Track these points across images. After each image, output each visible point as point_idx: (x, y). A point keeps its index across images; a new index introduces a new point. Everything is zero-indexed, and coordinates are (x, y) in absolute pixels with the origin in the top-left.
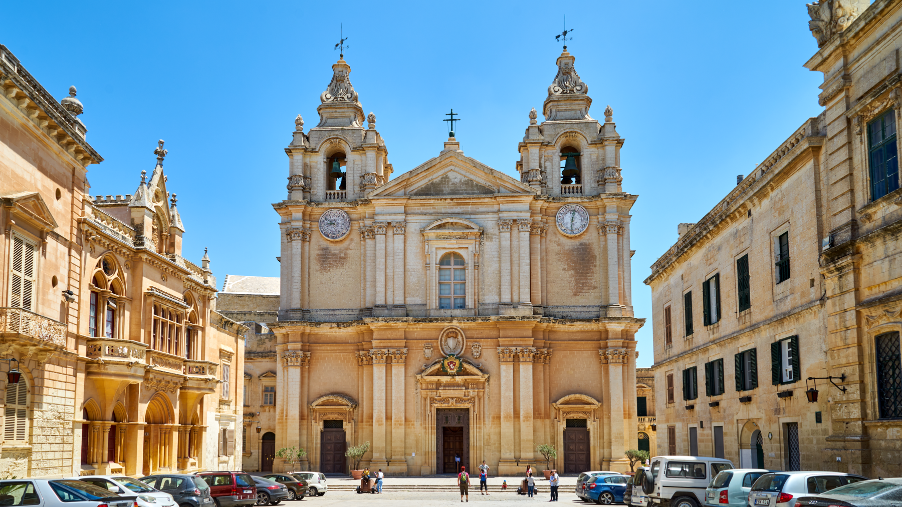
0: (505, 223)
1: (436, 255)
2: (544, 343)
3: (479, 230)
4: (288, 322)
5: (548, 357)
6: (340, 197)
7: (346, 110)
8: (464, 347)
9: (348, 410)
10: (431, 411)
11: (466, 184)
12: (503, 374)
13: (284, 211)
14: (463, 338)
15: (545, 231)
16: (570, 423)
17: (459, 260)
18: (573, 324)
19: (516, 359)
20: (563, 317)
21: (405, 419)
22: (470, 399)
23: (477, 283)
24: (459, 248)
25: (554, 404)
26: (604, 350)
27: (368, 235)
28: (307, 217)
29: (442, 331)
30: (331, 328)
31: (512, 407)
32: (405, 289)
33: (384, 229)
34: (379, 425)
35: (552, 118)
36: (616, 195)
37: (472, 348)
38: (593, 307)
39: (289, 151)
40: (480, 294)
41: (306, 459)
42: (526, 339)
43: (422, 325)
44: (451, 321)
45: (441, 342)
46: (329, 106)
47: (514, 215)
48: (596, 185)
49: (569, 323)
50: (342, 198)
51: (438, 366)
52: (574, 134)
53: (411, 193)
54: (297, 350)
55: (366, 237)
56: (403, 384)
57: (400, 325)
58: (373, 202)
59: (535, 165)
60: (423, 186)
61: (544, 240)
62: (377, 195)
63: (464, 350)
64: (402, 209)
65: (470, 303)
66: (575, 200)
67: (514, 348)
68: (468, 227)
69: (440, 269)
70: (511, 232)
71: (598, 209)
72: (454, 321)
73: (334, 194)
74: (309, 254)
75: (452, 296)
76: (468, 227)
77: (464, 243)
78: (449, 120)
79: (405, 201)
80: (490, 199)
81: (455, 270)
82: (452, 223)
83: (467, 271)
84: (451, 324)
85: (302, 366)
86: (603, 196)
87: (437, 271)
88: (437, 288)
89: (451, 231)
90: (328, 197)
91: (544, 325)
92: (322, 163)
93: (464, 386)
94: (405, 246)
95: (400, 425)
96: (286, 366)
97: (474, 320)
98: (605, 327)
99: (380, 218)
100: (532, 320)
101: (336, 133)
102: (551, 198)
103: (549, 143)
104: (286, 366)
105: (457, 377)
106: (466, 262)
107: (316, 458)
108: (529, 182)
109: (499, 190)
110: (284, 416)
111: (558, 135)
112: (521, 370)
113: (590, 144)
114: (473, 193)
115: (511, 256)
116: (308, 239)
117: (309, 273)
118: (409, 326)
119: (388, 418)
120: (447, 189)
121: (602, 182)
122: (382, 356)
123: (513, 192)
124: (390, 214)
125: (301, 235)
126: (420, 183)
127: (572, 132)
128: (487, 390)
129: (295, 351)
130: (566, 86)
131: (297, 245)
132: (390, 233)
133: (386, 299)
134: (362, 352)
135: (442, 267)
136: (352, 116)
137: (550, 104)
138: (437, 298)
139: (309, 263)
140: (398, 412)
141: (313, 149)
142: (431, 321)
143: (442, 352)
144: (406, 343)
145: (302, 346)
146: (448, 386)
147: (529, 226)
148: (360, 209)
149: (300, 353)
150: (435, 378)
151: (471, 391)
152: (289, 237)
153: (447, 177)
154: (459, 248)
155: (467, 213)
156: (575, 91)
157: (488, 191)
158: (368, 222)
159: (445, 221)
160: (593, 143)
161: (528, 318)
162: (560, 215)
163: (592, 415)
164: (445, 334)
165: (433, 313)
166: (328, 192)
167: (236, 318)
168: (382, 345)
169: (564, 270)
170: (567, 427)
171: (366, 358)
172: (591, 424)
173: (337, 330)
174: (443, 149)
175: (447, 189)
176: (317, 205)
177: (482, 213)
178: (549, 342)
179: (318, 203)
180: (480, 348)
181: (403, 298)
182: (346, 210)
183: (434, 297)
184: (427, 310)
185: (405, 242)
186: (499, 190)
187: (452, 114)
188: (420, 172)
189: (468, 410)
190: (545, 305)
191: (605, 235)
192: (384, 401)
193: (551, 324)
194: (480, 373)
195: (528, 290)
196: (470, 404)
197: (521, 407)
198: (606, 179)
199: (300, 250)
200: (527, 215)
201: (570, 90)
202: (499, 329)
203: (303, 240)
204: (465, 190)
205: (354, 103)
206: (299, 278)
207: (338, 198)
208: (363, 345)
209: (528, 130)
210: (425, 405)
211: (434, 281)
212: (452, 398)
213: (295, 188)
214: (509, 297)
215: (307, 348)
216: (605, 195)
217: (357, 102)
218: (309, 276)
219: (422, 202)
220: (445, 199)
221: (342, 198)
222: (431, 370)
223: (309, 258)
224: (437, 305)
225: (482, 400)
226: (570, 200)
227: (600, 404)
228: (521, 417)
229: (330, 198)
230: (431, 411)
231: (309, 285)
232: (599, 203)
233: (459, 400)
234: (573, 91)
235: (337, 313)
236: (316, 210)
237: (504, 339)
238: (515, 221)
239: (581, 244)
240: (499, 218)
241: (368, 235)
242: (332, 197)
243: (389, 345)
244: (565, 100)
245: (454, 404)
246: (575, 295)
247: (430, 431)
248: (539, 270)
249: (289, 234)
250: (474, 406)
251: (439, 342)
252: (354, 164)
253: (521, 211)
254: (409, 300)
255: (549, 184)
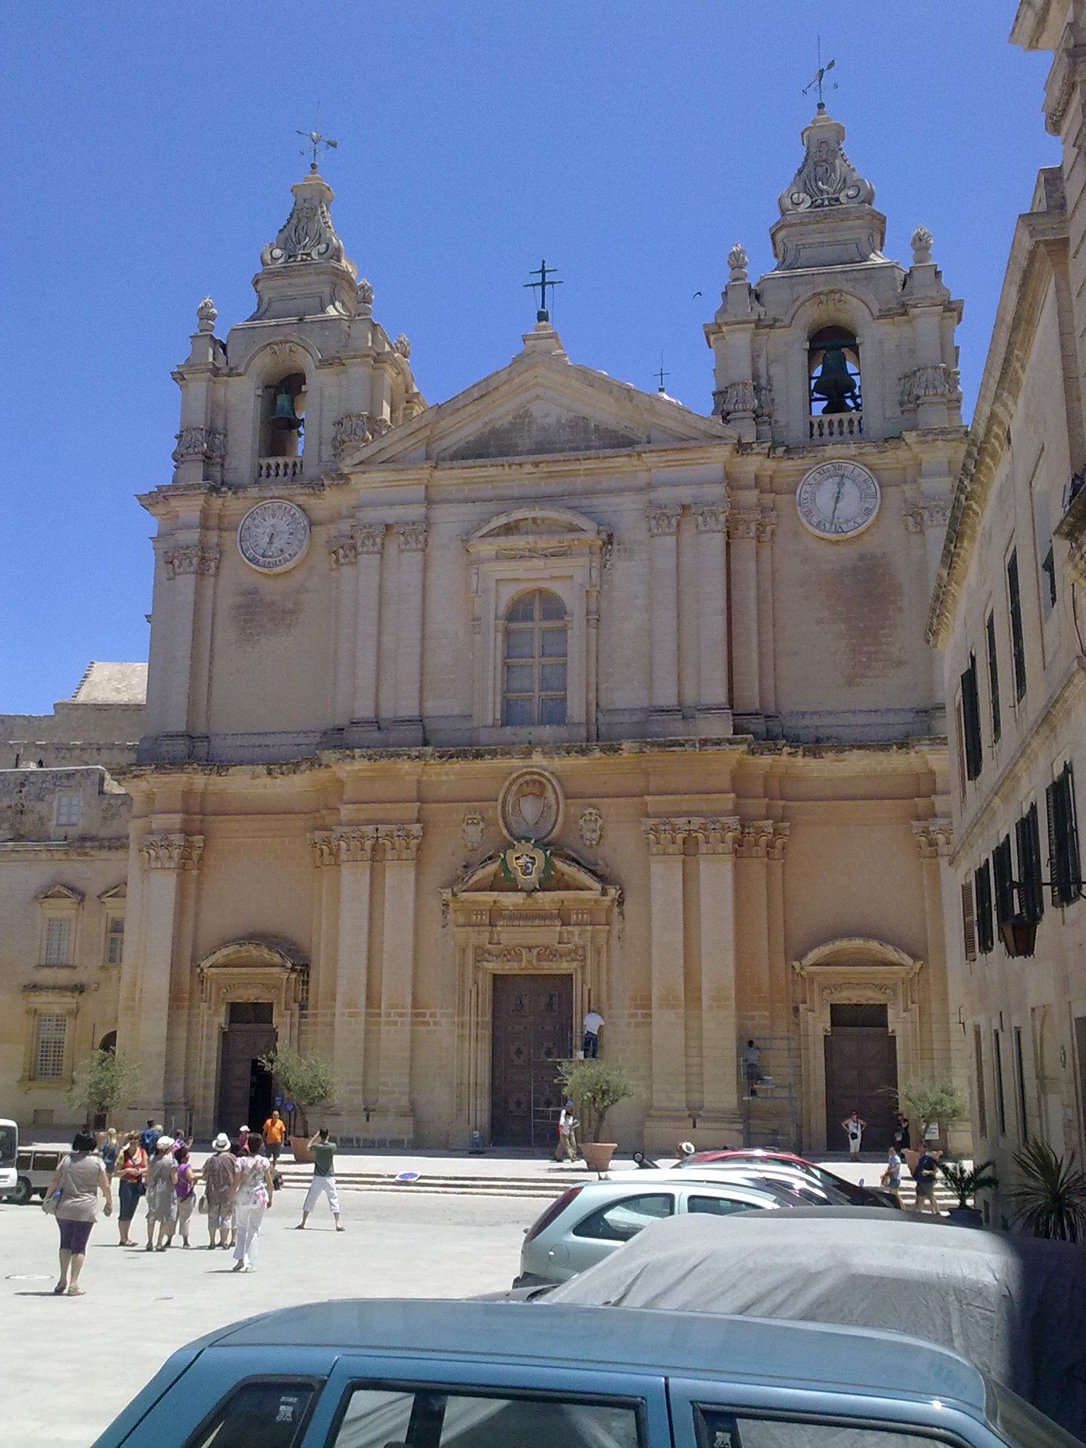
0: (664, 514)
1: (497, 597)
2: (768, 807)
3: (598, 533)
4: (151, 765)
5: (779, 843)
6: (290, 471)
7: (312, 279)
8: (560, 819)
9: (285, 976)
10: (476, 982)
11: (570, 427)
12: (657, 885)
13: (161, 509)
14: (557, 798)
15: (768, 529)
16: (841, 1016)
17: (553, 608)
18: (841, 756)
19: (689, 848)
20: (818, 740)
21: (414, 999)
22: (575, 951)
23: (593, 661)
24: (553, 578)
25: (796, 964)
26: (923, 823)
27: (346, 556)
28: (213, 522)
29: (506, 779)
30: (255, 776)
31: (681, 971)
32: (421, 681)
33: (378, 540)
34: (351, 1015)
35: (787, 263)
36: (943, 432)
37: (581, 822)
38: (895, 711)
39: (179, 377)
40: (603, 686)
41: (183, 1100)
42: (715, 796)
43: (458, 765)
44: (527, 754)
45: (503, 807)
46: (273, 274)
47: (685, 494)
48: (898, 411)
49: (831, 755)
50: (294, 473)
51: (492, 867)
52: (837, 296)
53: (442, 455)
54: (171, 831)
55: (342, 560)
56: (411, 913)
57: (405, 766)
58: (352, 477)
59: (743, 372)
60: (471, 438)
61: (766, 552)
62: (361, 463)
63: (558, 826)
64: (420, 492)
65: (576, 708)
66: (840, 450)
67: (684, 820)
68: (572, 529)
69: (508, 633)
70: (678, 533)
71: (904, 469)
72: (533, 756)
73: (278, 466)
74: (214, 604)
75: (537, 694)
76: (572, 529)
77: (562, 566)
78: (539, 284)
79: (424, 474)
80: (626, 459)
81: (546, 631)
82: (534, 520)
83: (569, 632)
84: (528, 762)
85: (183, 869)
86: (910, 437)
87: (500, 636)
88: (499, 676)
89: (530, 538)
90: (261, 475)
91: (766, 760)
92: (252, 400)
93: (559, 916)
94: (425, 579)
95: (401, 1015)
96: (146, 872)
97: (583, 752)
98: (926, 763)
99: (370, 515)
100: (727, 747)
101: (286, 330)
102: (782, 447)
103: (776, 320)
104: (146, 872)
105: (540, 894)
106: (568, 610)
107: (205, 1098)
108: (728, 414)
109: (648, 437)
110: (138, 990)
111: (798, 304)
112: (703, 876)
113: (880, 317)
114: (588, 448)
115: (678, 593)
116: (212, 571)
117: (212, 650)
118: (427, 768)
119: (372, 999)
120: (525, 442)
121: (910, 403)
122: (362, 844)
123: (682, 440)
124: (391, 504)
125: (195, 561)
126: (466, 429)
127: (832, 292)
128: (616, 927)
129: (168, 832)
130: (821, 191)
131: (186, 583)
132: (392, 549)
133: (377, 706)
134: (319, 835)
135: (513, 626)
136: (327, 290)
137: (783, 233)
138: (499, 699)
139: (213, 623)
140: (396, 986)
141: (231, 369)
142: (478, 756)
143: (505, 832)
144: (419, 810)
145: (185, 821)
146: (519, 918)
147: (722, 518)
148: (332, 499)
149: (177, 839)
150: (488, 897)
151: (576, 930)
152: (171, 566)
153: (527, 414)
154: (553, 578)
155: (571, 494)
156: (843, 199)
157: (620, 442)
158: (345, 526)
159: (517, 515)
160: (885, 314)
161: (718, 744)
162: (807, 488)
163: (900, 994)
164: (514, 788)
165: (484, 736)
166: (264, 462)
167: (79, 758)
168: (362, 816)
169: (820, 621)
170: (833, 1025)
171: (330, 849)
172: (897, 1016)
173: (268, 780)
174: (520, 347)
175: (525, 442)
176: (235, 493)
177: (609, 492)
178: (782, 803)
179: (236, 488)
180: (600, 821)
181: (416, 703)
182: (301, 500)
183: (490, 698)
184: (473, 729)
185: (425, 568)
186: (648, 437)
187: (543, 272)
188: (462, 404)
189: (568, 978)
190: (771, 710)
191: (922, 532)
192: (364, 956)
193: (784, 758)
194: (597, 886)
195: (720, 675)
196: (575, 964)
197: (704, 970)
198: (918, 398)
199: (191, 598)
200: (719, 491)
201: (829, 199)
202: (646, 774)
203: (201, 573)
204: (569, 440)
205: (333, 263)
206: (188, 662)
207: (285, 474)
208: (323, 817)
209: (725, 294)
210: (463, 964)
211: (491, 660)
212: (530, 948)
213: (188, 457)
214: (673, 692)
215: (197, 826)
216: (914, 433)
217: (339, 261)
218: (211, 657)
219: (468, 473)
220: (520, 465)
221: (294, 473)
222: (475, 878)
223: (214, 614)
224: (498, 716)
225: (604, 955)
226: (830, 451)
227: (919, 964)
228: (705, 998)
229: (268, 475)
230: (476, 982)
231: (210, 678)
232: (902, 454)
233: (549, 953)
234: (837, 200)
235: (270, 740)
236: (232, 504)
237: (658, 798)
238: (685, 508)
239: (862, 557)
240: (650, 502)
241: (346, 556)
242: (273, 473)
243: (380, 816)
244: (818, 222)
245: (534, 962)
246: (850, 683)
247: (473, 1032)
248: (754, 626)
249: (169, 560)
250: (583, 967)
251: (499, 807)
252: (321, 396)
253: (700, 483)
254: (433, 707)
255: (780, 417)
